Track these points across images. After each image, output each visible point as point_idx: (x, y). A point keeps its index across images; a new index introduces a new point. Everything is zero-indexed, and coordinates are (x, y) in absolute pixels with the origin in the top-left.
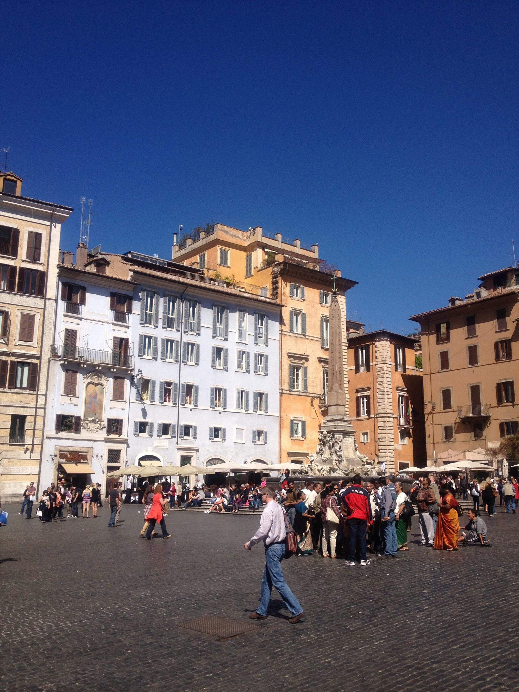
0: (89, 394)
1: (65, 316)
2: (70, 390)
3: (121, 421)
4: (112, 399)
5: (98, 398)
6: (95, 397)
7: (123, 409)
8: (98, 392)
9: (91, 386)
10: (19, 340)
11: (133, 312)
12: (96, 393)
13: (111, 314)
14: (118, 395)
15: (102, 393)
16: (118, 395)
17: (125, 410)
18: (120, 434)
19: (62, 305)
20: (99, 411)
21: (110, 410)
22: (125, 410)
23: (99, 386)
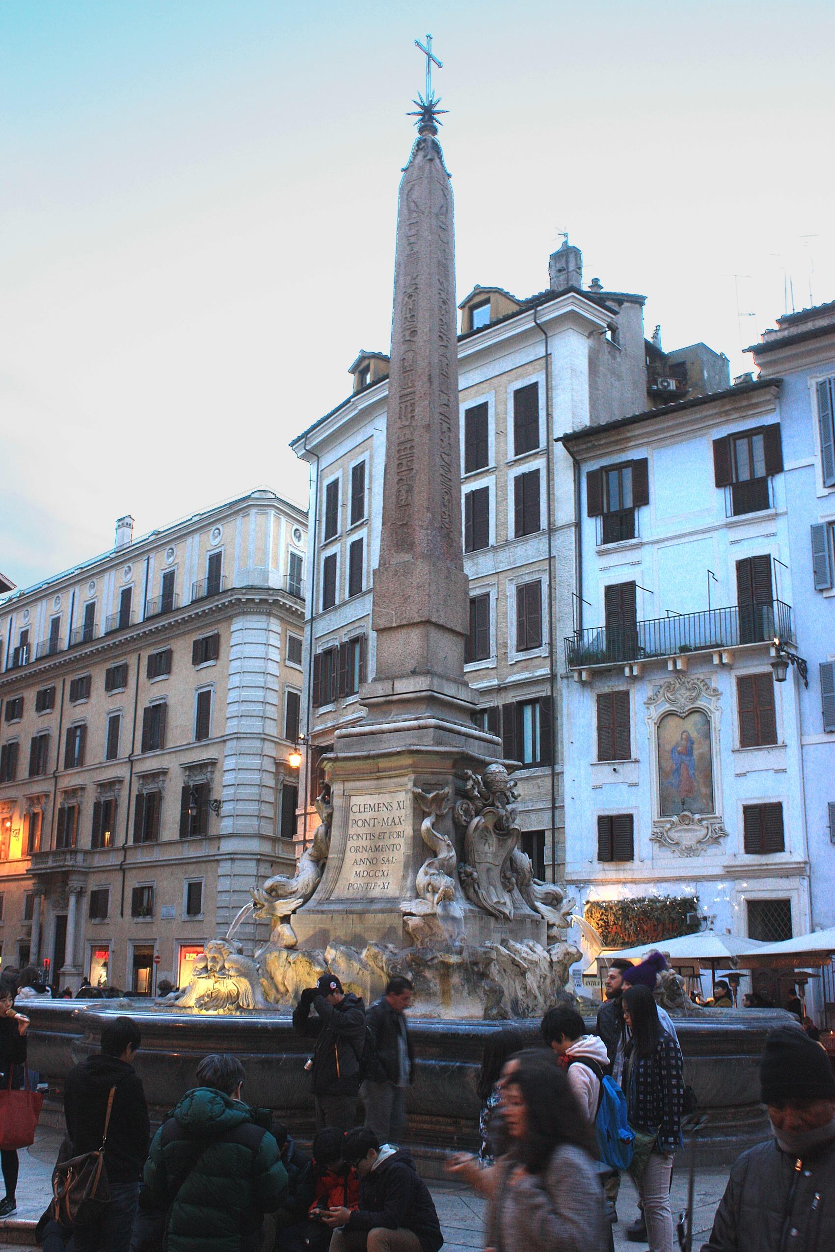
0: (668, 747)
1: (600, 553)
2: (614, 745)
3: (778, 807)
4: (737, 745)
5: (696, 752)
6: (689, 752)
7: (777, 771)
8: (694, 735)
9: (672, 722)
10: (518, 651)
11: (787, 466)
12: (690, 741)
13: (720, 500)
14: (758, 729)
15: (708, 736)
16: (758, 729)
17: (784, 771)
18: (780, 848)
19: (592, 528)
20: (704, 790)
21: (740, 780)
22: (784, 771)
23: (696, 717)
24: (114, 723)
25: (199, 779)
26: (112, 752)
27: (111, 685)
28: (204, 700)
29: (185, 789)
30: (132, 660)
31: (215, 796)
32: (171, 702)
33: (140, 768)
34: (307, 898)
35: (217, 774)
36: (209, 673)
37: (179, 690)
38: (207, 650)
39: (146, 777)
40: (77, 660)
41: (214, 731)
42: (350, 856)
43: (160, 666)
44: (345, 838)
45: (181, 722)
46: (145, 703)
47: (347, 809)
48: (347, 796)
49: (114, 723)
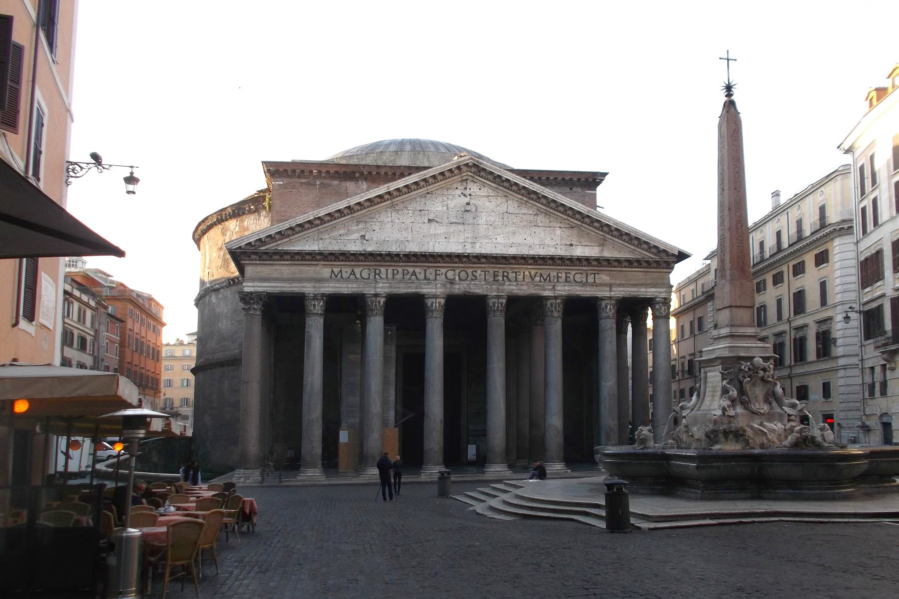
24: (779, 302)
25: (824, 327)
26: (780, 318)
27: (775, 283)
28: (823, 285)
29: (818, 334)
30: (784, 268)
31: (833, 336)
32: (806, 289)
33: (794, 324)
34: (692, 410)
35: (833, 324)
36: (825, 270)
37: (809, 281)
38: (822, 259)
39: (798, 329)
40: (774, 263)
41: (830, 301)
42: (707, 394)
43: (799, 269)
44: (705, 388)
45: (813, 298)
46: (793, 290)
47: (706, 377)
48: (706, 373)
49: (779, 302)
